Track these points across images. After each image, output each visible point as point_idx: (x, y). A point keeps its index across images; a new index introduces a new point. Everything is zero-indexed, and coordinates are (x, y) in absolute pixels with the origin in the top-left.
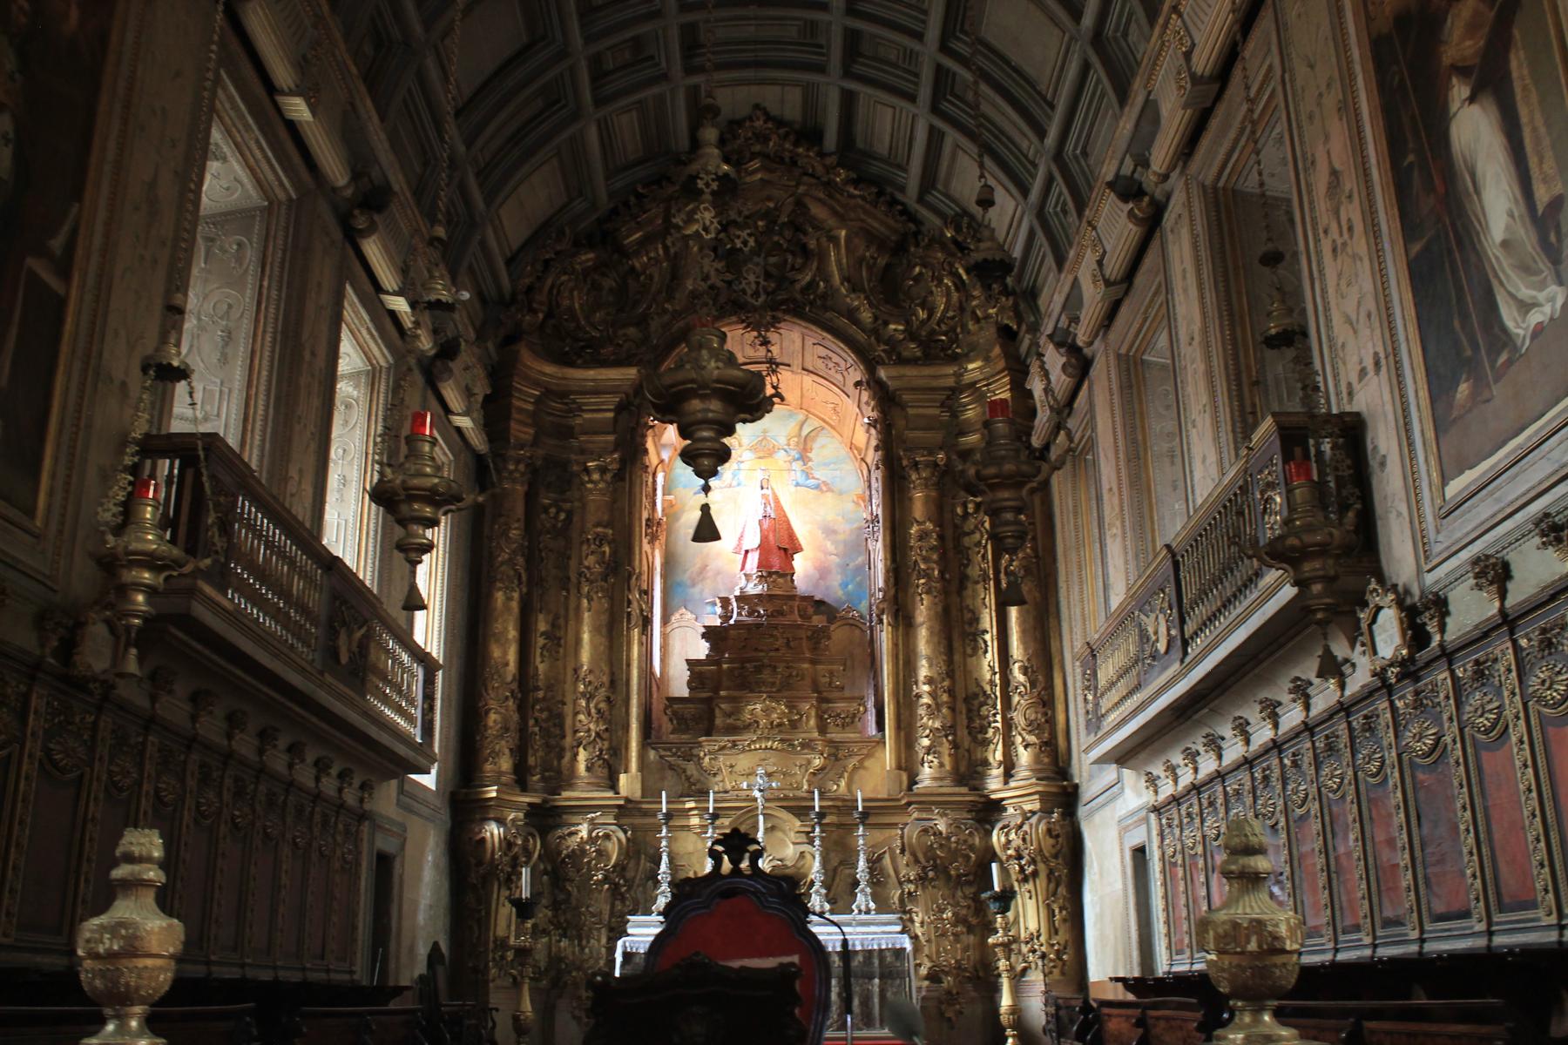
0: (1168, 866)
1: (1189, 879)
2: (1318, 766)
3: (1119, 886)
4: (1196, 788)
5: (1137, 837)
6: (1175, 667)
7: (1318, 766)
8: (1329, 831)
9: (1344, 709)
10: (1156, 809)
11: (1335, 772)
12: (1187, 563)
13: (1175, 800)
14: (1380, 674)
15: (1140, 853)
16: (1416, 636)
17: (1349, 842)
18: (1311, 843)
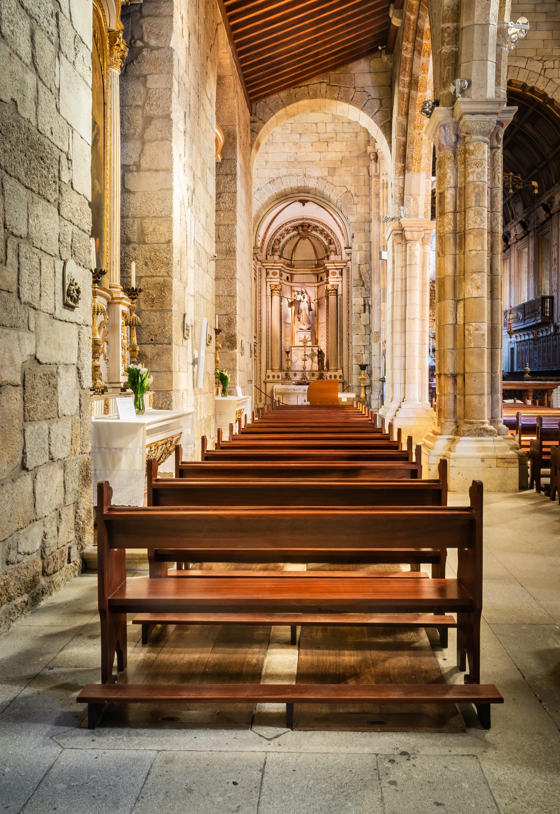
0: (518, 352)
1: (522, 356)
2: (543, 342)
3: (507, 354)
4: (524, 341)
5: (512, 346)
6: (522, 323)
7: (543, 342)
8: (544, 352)
9: (547, 336)
10: (517, 342)
11: (545, 344)
12: (526, 306)
13: (521, 342)
14: (551, 334)
15: (512, 349)
16: (555, 331)
17: (546, 355)
18: (541, 354)
